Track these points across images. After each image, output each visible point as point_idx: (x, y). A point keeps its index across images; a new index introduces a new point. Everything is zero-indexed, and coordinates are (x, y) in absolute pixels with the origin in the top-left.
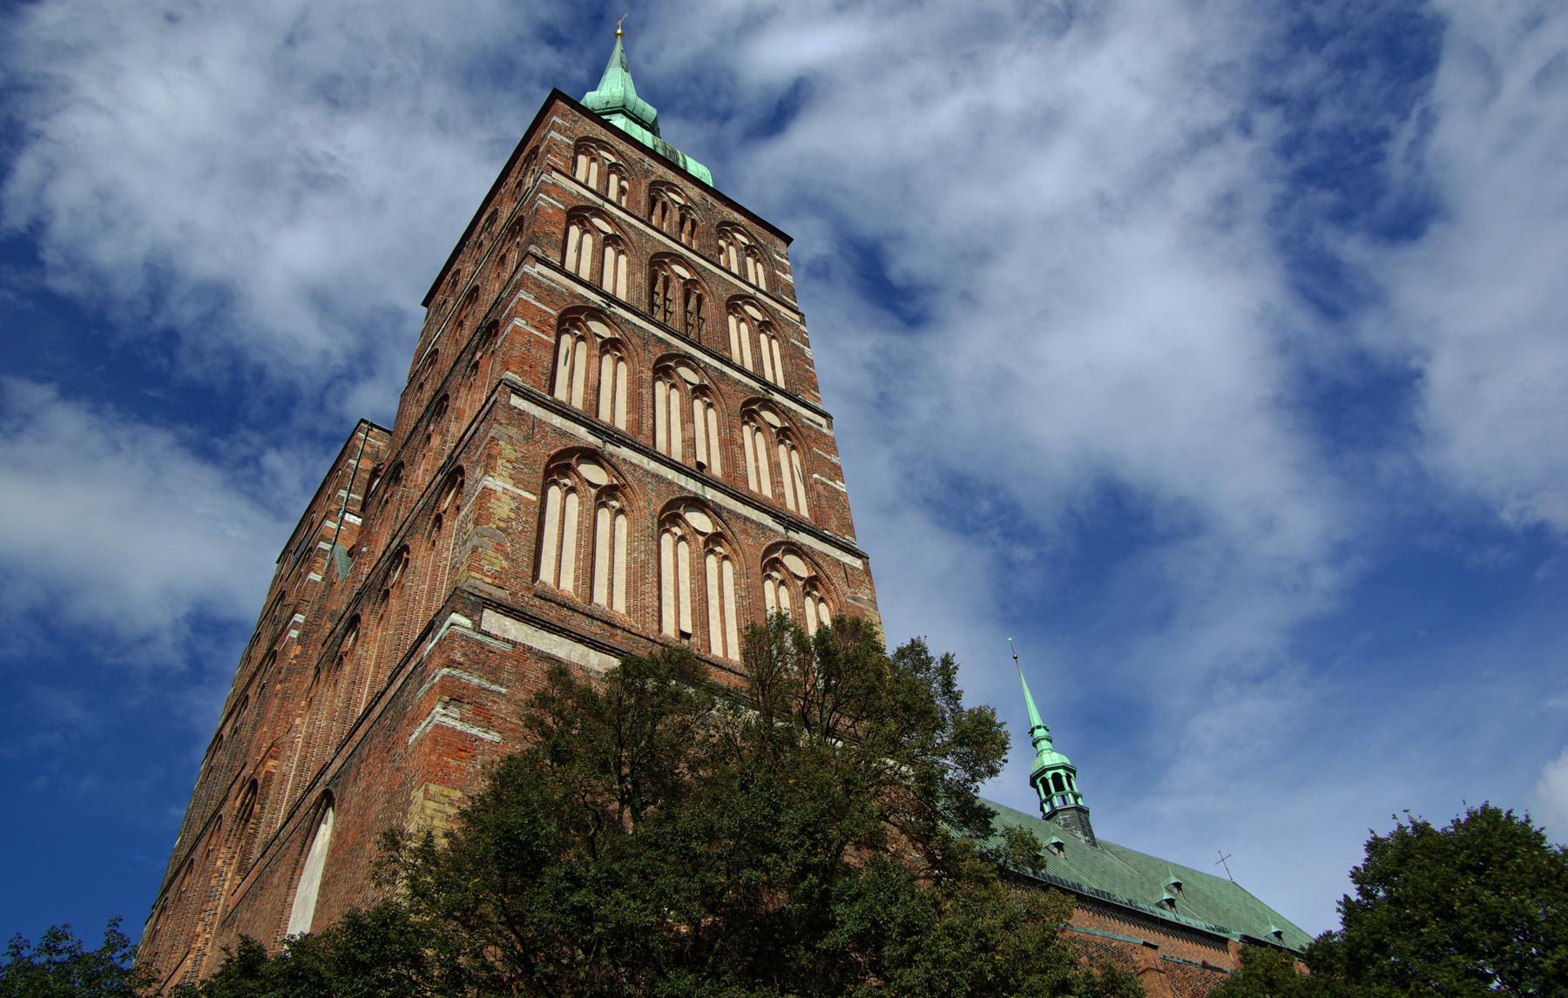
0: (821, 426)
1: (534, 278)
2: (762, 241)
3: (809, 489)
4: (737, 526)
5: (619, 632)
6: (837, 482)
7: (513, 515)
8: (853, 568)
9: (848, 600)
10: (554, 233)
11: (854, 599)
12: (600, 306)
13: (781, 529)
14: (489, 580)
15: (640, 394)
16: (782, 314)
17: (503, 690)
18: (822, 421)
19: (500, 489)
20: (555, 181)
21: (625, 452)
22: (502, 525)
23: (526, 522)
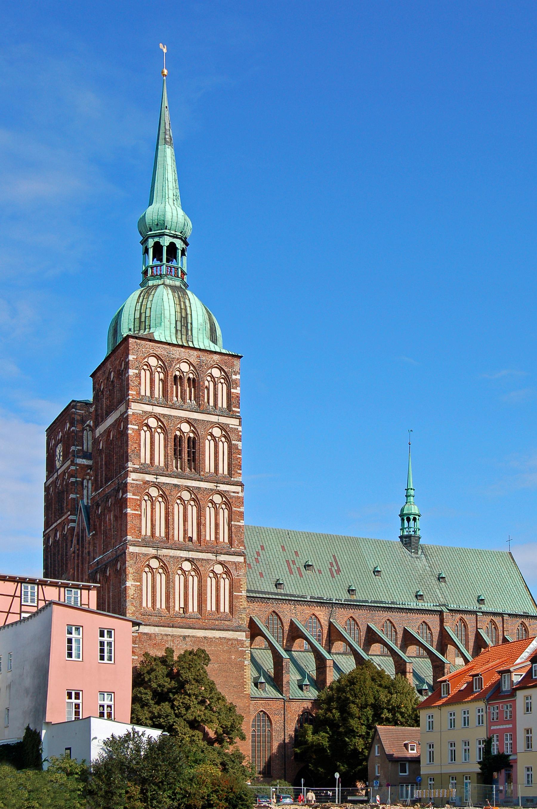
0: (238, 493)
1: (132, 484)
2: (226, 370)
3: (230, 529)
4: (199, 564)
5: (163, 618)
7: (134, 593)
8: (239, 563)
10: (136, 448)
12: (154, 482)
14: (131, 615)
15: (168, 519)
16: (231, 426)
17: (137, 646)
18: (239, 489)
19: (130, 585)
20: (133, 411)
21: (165, 552)
22: (132, 597)
23: (138, 593)
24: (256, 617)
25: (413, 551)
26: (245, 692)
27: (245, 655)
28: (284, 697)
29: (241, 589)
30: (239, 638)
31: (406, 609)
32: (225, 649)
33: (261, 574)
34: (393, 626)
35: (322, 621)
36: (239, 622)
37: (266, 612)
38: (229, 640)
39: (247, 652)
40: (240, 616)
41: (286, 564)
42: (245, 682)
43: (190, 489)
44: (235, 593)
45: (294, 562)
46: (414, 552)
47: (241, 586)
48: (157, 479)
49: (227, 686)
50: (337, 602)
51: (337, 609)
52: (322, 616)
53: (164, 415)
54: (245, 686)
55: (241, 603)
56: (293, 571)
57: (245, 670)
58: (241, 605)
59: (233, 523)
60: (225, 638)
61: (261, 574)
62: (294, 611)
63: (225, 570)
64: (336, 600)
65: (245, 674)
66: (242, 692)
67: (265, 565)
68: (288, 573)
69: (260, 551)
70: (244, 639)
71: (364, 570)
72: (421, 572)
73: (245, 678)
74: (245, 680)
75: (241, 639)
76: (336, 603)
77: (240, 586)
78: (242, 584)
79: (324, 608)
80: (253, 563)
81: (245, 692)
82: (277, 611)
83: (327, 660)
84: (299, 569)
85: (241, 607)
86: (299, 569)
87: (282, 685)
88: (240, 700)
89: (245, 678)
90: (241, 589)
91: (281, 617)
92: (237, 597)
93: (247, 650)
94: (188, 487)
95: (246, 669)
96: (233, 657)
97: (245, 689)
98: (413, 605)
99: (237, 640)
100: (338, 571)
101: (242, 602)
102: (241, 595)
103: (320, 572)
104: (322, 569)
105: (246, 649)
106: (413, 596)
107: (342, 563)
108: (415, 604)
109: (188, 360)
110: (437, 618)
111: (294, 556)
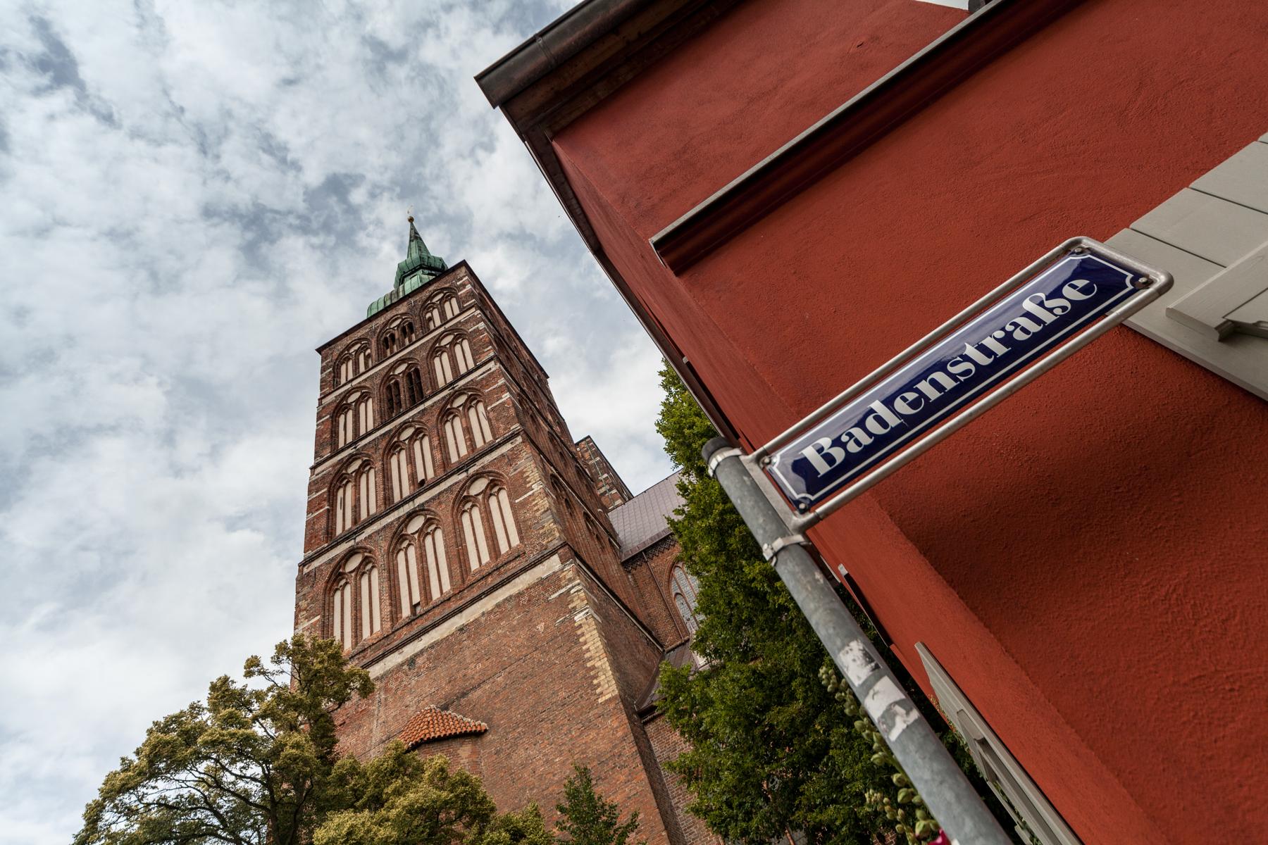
6: (503, 396)
11: (515, 470)
13: (464, 475)
42: (593, 668)
43: (409, 422)
48: (355, 448)
49: (544, 715)
53: (365, 380)
54: (595, 682)
59: (489, 408)
66: (593, 705)
73: (589, 659)
74: (589, 665)
85: (538, 514)
88: (593, 734)
89: (589, 659)
94: (405, 423)
95: (583, 634)
97: (598, 691)
109: (397, 315)
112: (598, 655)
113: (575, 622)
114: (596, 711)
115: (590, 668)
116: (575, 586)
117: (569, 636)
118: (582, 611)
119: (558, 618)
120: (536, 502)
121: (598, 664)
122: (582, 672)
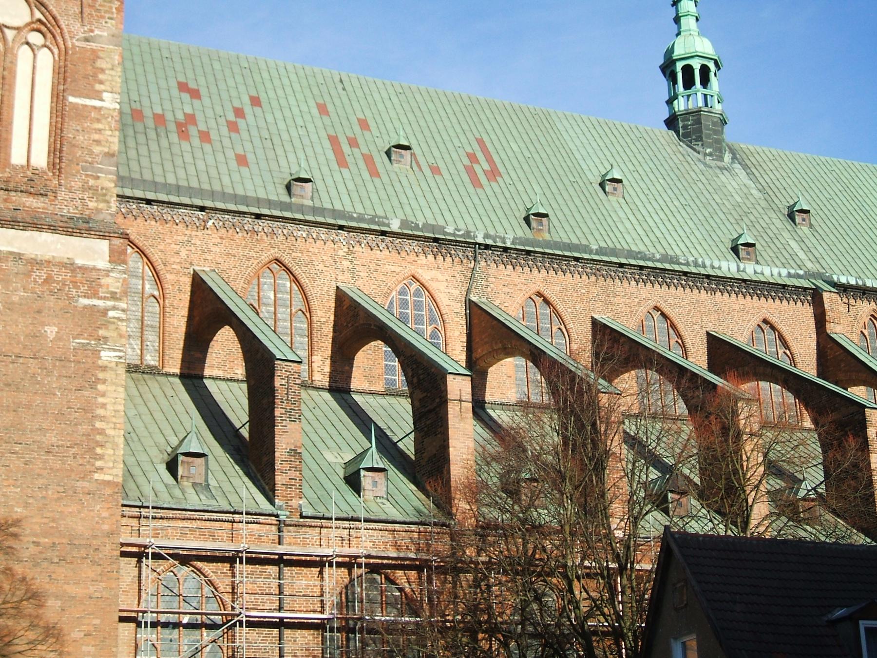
9: (77, 44)
11: (87, 40)
24: (213, 275)
25: (708, 151)
26: (96, 476)
27: (105, 325)
28: (280, 508)
29: (98, 87)
30: (79, 262)
31: (708, 277)
32: (15, 299)
33: (242, 160)
34: (673, 326)
35: (443, 300)
36: (84, 205)
37: (249, 259)
38: (36, 263)
39: (111, 314)
40: (91, 182)
41: (327, 144)
42: (102, 432)
44: (71, 99)
45: (353, 143)
46: (710, 154)
47: (101, 76)
49: (17, 448)
50: (490, 242)
51: (493, 265)
52: (442, 286)
54: (99, 450)
55: (96, 137)
56: (350, 160)
57: (100, 387)
58: (98, 142)
60: (18, 257)
61: (242, 160)
62: (346, 263)
63: (38, 15)
64: (487, 236)
65: (101, 400)
66: (85, 476)
67: (257, 142)
68: (334, 166)
69: (248, 109)
70: (103, 263)
71: (572, 179)
72: (739, 200)
73: (102, 418)
74: (98, 425)
75: (90, 263)
76: (487, 247)
77: (94, 76)
78: (102, 71)
79: (449, 259)
80: (220, 132)
81: (96, 476)
82: (286, 260)
83: (450, 378)
84: (369, 160)
85: (97, 149)
86: (369, 160)
87: (273, 464)
88: (73, 508)
89: (102, 418)
90: (98, 87)
91: (304, 280)
92: (81, 113)
93: (114, 308)
95: (104, 381)
96: (51, 331)
97: (99, 464)
98: (728, 267)
99: (70, 266)
100: (493, 174)
101: (100, 131)
102: (99, 109)
103: (435, 170)
104: (441, 165)
105: (110, 303)
106: (724, 250)
107: (504, 157)
108: (733, 268)
110: (805, 312)
111: (357, 128)
112: (114, 420)
113: (100, 358)
114: (86, 484)
115: (98, 429)
116: (117, 309)
117: (87, 371)
118: (114, 350)
119: (79, 336)
120: (100, 126)
121: (110, 432)
122: (84, 428)
